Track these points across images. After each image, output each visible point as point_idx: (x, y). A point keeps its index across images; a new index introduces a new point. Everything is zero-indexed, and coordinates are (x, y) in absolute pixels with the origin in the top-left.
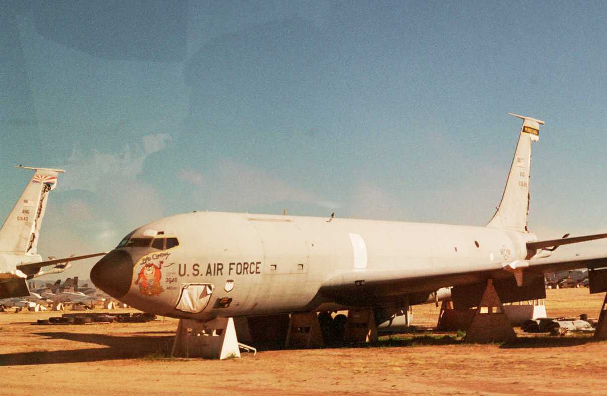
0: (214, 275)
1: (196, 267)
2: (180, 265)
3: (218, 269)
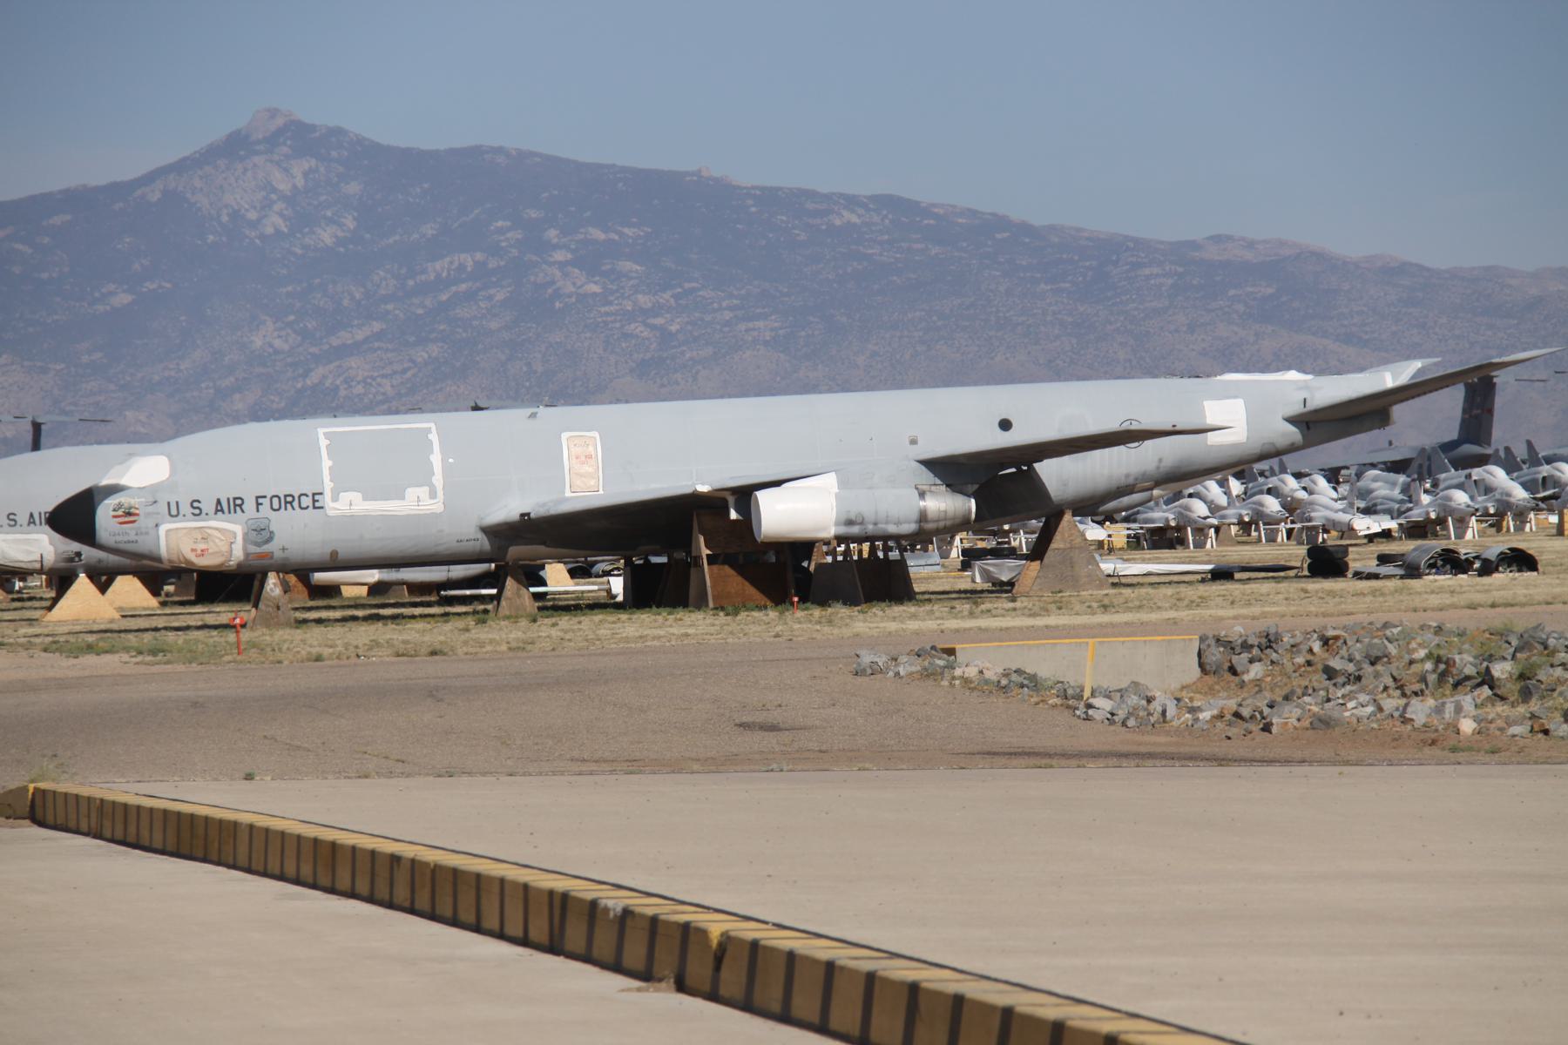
0: (230, 512)
2: (169, 503)
3: (235, 505)
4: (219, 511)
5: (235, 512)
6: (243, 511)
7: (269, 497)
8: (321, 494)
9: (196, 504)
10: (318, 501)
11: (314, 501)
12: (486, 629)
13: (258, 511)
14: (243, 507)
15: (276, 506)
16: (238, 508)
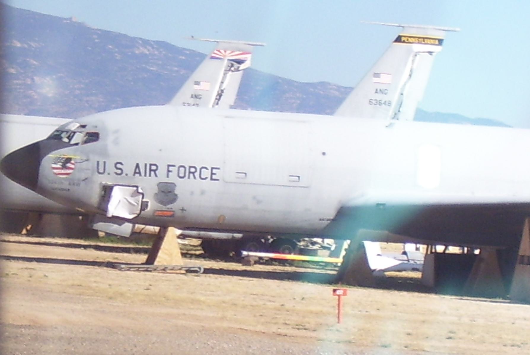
0: (145, 175)
1: (119, 166)
2: (98, 162)
3: (151, 170)
4: (137, 173)
5: (150, 175)
6: (156, 176)
7: (177, 166)
9: (119, 166)
10: (215, 174)
11: (212, 174)
12: (390, 294)
13: (168, 176)
14: (157, 172)
15: (182, 175)
16: (152, 173)
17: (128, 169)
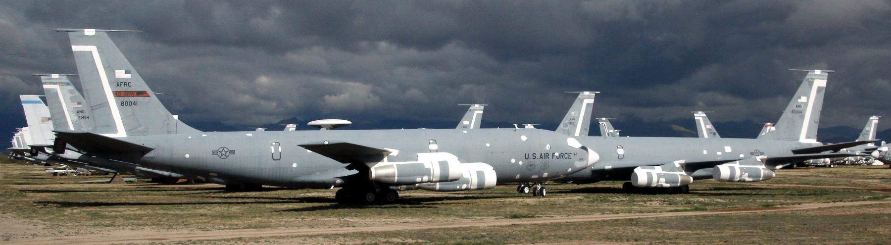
1: (534, 155)
3: (546, 156)
8: (571, 153)
9: (534, 155)
11: (569, 156)
17: (538, 156)
